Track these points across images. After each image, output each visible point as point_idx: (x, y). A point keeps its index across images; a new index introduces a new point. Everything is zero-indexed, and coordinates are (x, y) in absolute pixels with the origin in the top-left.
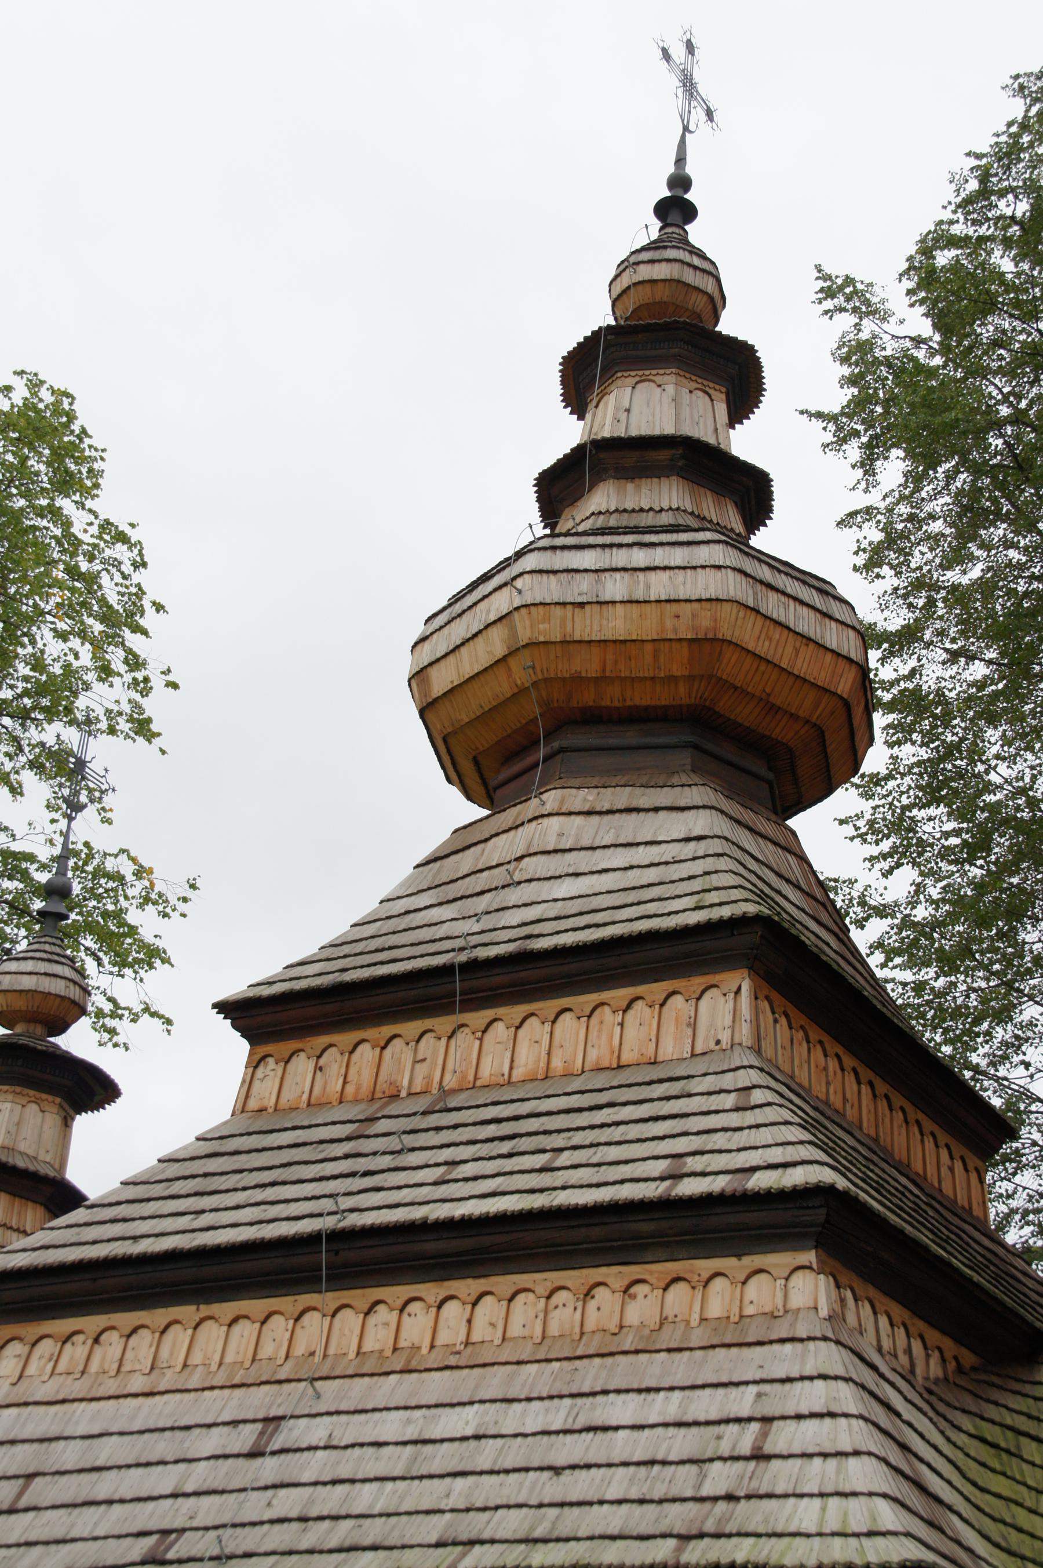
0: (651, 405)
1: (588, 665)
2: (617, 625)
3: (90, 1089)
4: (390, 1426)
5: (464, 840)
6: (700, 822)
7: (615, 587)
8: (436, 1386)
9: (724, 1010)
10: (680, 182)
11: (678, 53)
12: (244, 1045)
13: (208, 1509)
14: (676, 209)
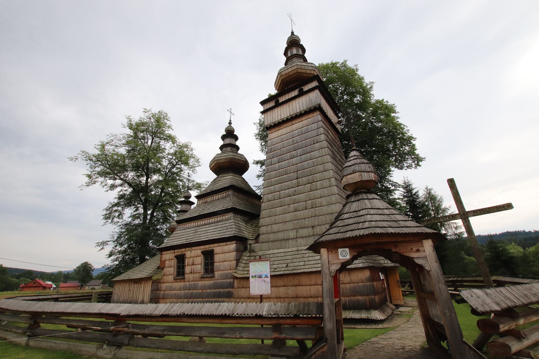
0: (228, 141)
2: (223, 161)
7: (222, 158)
8: (208, 226)
9: (230, 192)
10: (230, 121)
11: (230, 110)
14: (230, 123)
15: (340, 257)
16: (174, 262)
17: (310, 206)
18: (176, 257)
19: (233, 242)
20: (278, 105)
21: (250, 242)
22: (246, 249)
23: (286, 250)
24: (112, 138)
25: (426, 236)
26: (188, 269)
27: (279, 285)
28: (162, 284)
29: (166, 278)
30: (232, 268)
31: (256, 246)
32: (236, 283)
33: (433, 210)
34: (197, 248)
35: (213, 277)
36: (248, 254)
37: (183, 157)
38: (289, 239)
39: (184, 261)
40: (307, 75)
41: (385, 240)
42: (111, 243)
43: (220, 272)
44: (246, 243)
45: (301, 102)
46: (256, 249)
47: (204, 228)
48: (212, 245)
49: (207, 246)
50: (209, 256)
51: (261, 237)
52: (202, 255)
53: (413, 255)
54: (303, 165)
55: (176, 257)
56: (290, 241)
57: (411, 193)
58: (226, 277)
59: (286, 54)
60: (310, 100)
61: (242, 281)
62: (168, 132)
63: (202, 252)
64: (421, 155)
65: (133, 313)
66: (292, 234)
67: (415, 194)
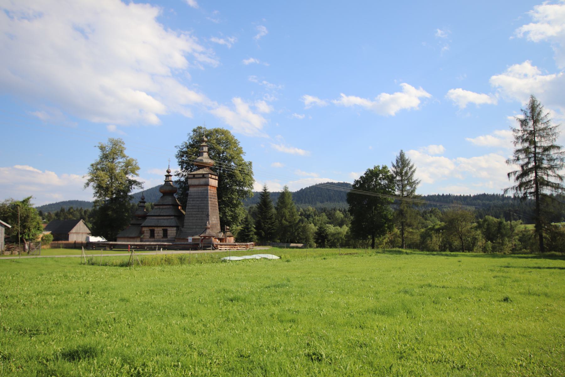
26: (156, 235)
31: (183, 229)
47: (162, 221)
58: (172, 238)
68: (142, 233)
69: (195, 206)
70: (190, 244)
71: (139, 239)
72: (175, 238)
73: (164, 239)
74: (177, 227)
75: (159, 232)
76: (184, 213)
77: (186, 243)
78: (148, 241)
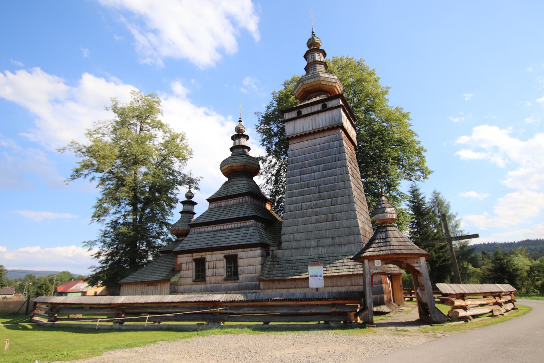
1: (235, 168)
2: (237, 164)
3: (195, 204)
4: (223, 235)
5: (226, 183)
6: (245, 182)
8: (227, 231)
12: (208, 203)
13: (210, 242)
15: (376, 265)
16: (193, 265)
17: (331, 219)
18: (195, 260)
19: (258, 248)
20: (300, 116)
21: (272, 248)
22: (268, 254)
23: (307, 257)
24: (101, 125)
25: (422, 255)
26: (208, 272)
27: (303, 286)
28: (179, 287)
29: (183, 281)
30: (257, 271)
31: (279, 253)
32: (262, 285)
33: (439, 217)
34: (219, 252)
35: (238, 279)
36: (271, 260)
37: (174, 148)
38: (310, 247)
39: (204, 265)
40: (329, 87)
41: (401, 256)
42: (97, 243)
43: (245, 276)
44: (268, 249)
45: (324, 118)
46: (279, 255)
48: (235, 251)
49: (230, 251)
50: (232, 261)
51: (284, 245)
52: (225, 260)
53: (414, 265)
54: (324, 180)
55: (195, 260)
56: (312, 249)
57: (418, 198)
58: (252, 279)
59: (306, 57)
60: (333, 118)
61: (268, 283)
62: (159, 117)
63: (226, 257)
64: (430, 168)
65: (229, 300)
66: (313, 243)
67: (421, 200)
68: (175, 270)
69: (308, 186)
70: (316, 298)
71: (167, 287)
72: (260, 280)
73: (231, 284)
74: (263, 246)
75: (216, 263)
76: (279, 219)
77: (298, 292)
78: (190, 292)
